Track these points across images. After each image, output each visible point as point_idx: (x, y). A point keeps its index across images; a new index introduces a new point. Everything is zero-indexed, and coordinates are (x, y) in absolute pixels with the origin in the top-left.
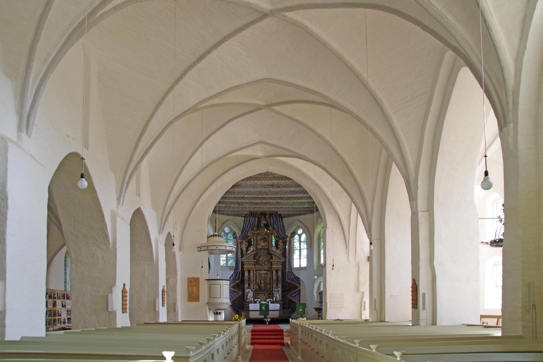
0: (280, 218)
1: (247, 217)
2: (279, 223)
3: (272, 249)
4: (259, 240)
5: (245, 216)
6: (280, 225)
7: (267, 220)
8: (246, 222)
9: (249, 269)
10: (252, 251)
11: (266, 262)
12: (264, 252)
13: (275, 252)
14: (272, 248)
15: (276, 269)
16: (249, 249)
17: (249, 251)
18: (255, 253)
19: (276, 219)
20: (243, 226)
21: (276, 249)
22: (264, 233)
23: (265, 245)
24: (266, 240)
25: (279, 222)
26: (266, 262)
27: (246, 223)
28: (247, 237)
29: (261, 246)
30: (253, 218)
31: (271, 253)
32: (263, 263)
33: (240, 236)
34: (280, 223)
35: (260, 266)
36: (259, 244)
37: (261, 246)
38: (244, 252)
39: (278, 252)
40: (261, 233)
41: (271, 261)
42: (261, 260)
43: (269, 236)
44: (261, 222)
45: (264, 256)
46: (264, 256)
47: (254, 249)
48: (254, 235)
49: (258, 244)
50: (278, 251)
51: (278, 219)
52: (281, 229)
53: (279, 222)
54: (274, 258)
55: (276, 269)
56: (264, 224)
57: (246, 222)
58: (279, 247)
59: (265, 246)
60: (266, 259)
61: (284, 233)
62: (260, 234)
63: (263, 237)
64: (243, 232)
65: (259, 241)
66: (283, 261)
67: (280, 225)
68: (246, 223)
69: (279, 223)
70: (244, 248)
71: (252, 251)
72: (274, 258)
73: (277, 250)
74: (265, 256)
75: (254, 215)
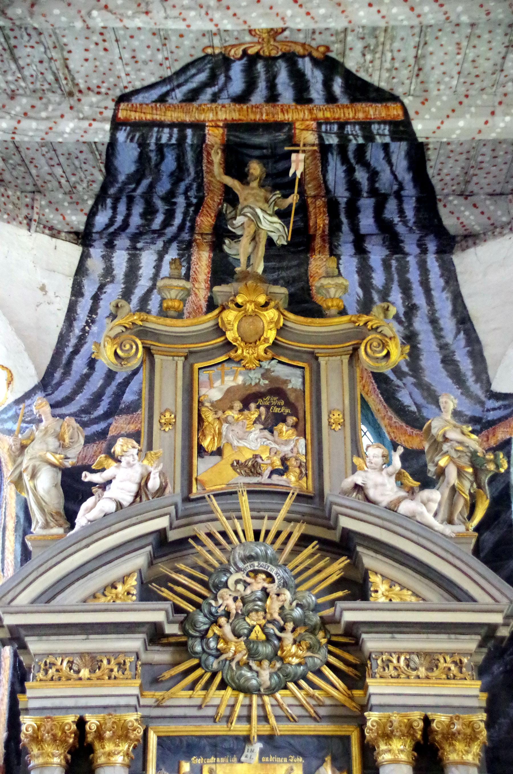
0: (424, 251)
1: (110, 246)
2: (419, 299)
3: (358, 479)
4: (216, 406)
5: (92, 215)
6: (434, 321)
7: (294, 199)
8: (101, 288)
9: (81, 723)
10: (127, 499)
11: (288, 637)
12: (264, 525)
13: (392, 508)
14: (354, 469)
15: (410, 726)
16: (87, 477)
17: (90, 501)
18: (163, 523)
19: (386, 265)
20: (62, 315)
21: (399, 477)
22: (271, 335)
23: (284, 460)
24: (295, 412)
25: (417, 291)
26: (288, 637)
27: (96, 298)
28: (102, 425)
29: (237, 466)
30: (173, 254)
31: (345, 522)
32: (252, 654)
33: (18, 401)
34: (430, 301)
35: (223, 686)
36: (219, 452)
37: (237, 466)
38: (37, 529)
39: (429, 518)
40: (230, 336)
41: (349, 617)
42: (233, 607)
43: (322, 361)
44: (240, 220)
45: (266, 558)
46: (266, 558)
47: (154, 483)
48: (158, 358)
49: (201, 451)
50: (425, 503)
51: (412, 261)
52: (443, 347)
53: (417, 291)
54: (383, 588)
55: (416, 716)
56: (270, 242)
57: (101, 288)
58: (442, 472)
59: (283, 471)
60: (287, 595)
61: (471, 381)
62: (228, 345)
63: (255, 377)
64: (67, 373)
65: (209, 416)
66: (497, 618)
67: (434, 321)
68: (96, 298)
69: (419, 299)
70: (33, 476)
71: (119, 506)
72: (383, 588)
73: (412, 492)
74: (273, 561)
75: (177, 221)
